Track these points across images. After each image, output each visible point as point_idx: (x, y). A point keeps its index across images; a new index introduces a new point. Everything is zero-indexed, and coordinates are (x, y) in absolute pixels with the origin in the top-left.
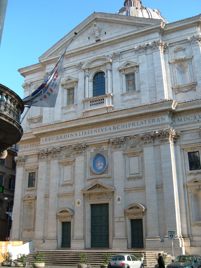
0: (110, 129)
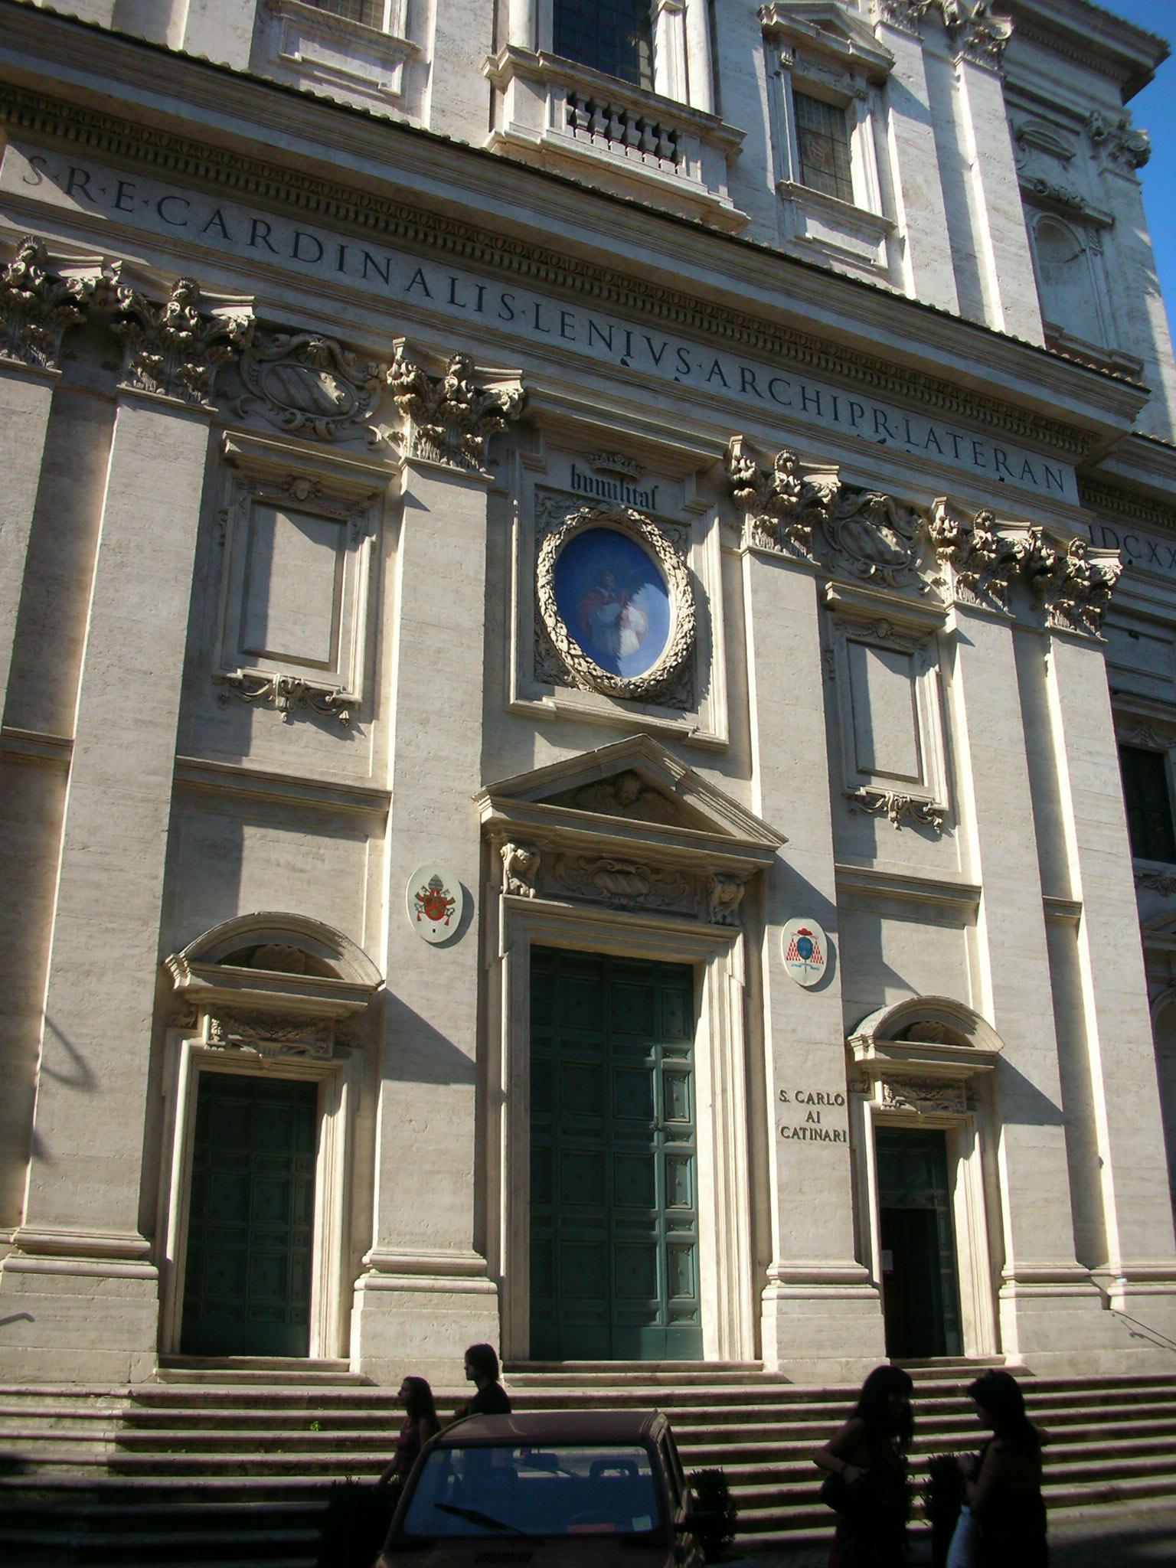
0: (716, 378)
